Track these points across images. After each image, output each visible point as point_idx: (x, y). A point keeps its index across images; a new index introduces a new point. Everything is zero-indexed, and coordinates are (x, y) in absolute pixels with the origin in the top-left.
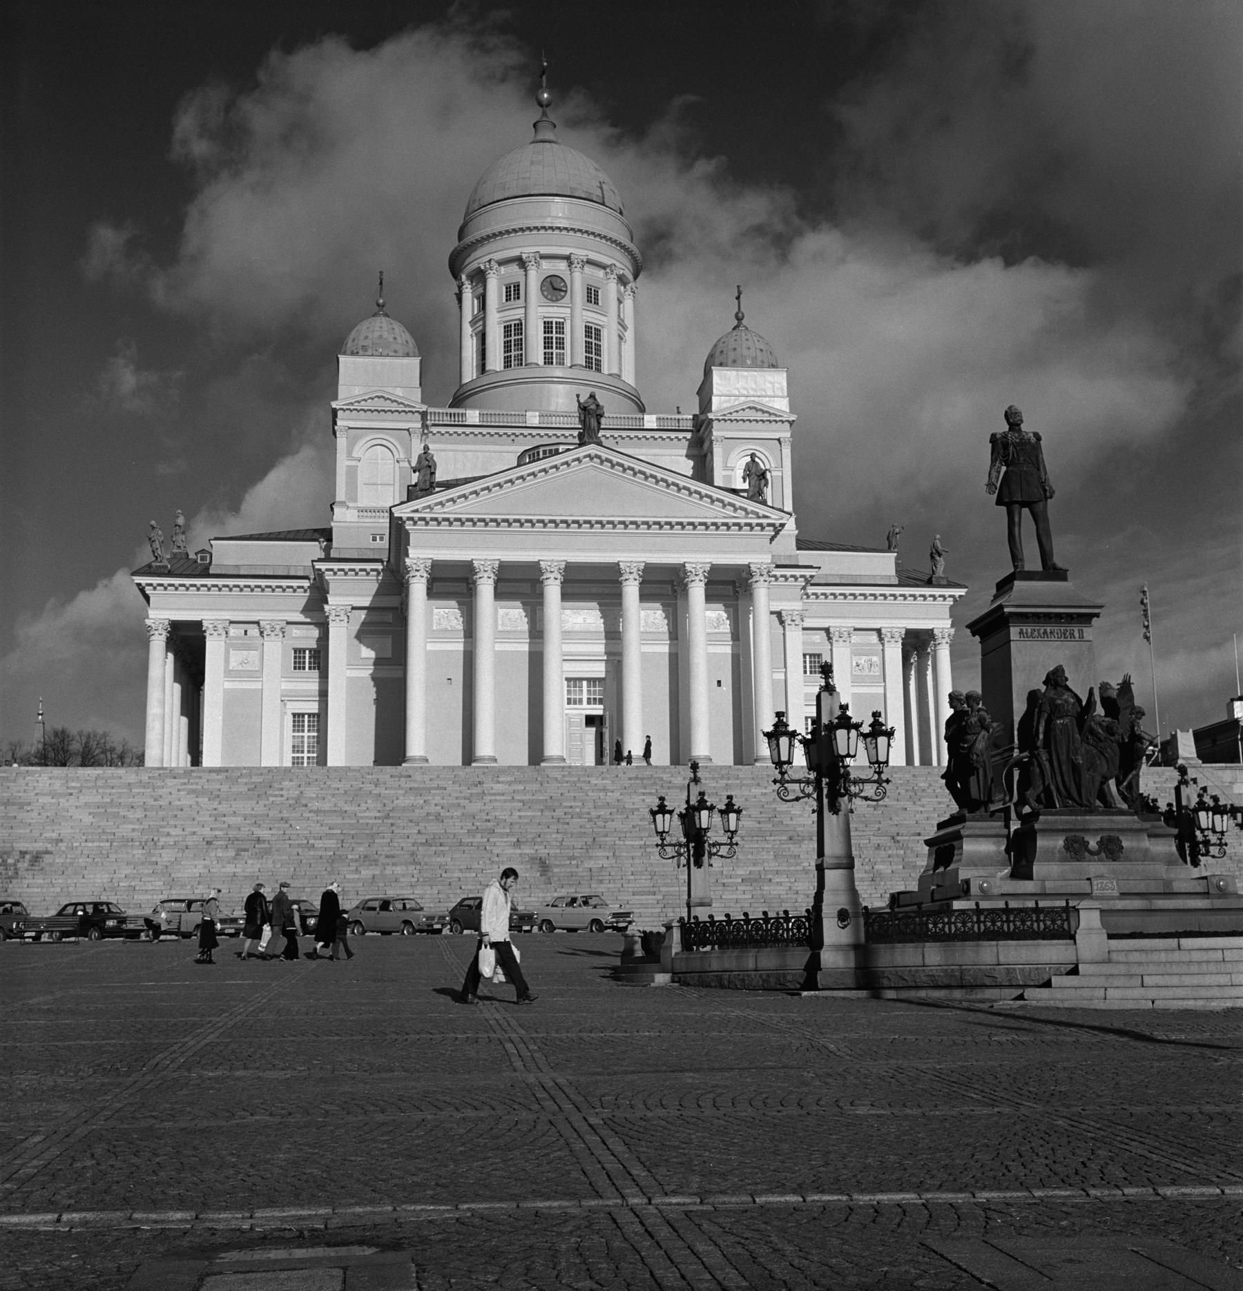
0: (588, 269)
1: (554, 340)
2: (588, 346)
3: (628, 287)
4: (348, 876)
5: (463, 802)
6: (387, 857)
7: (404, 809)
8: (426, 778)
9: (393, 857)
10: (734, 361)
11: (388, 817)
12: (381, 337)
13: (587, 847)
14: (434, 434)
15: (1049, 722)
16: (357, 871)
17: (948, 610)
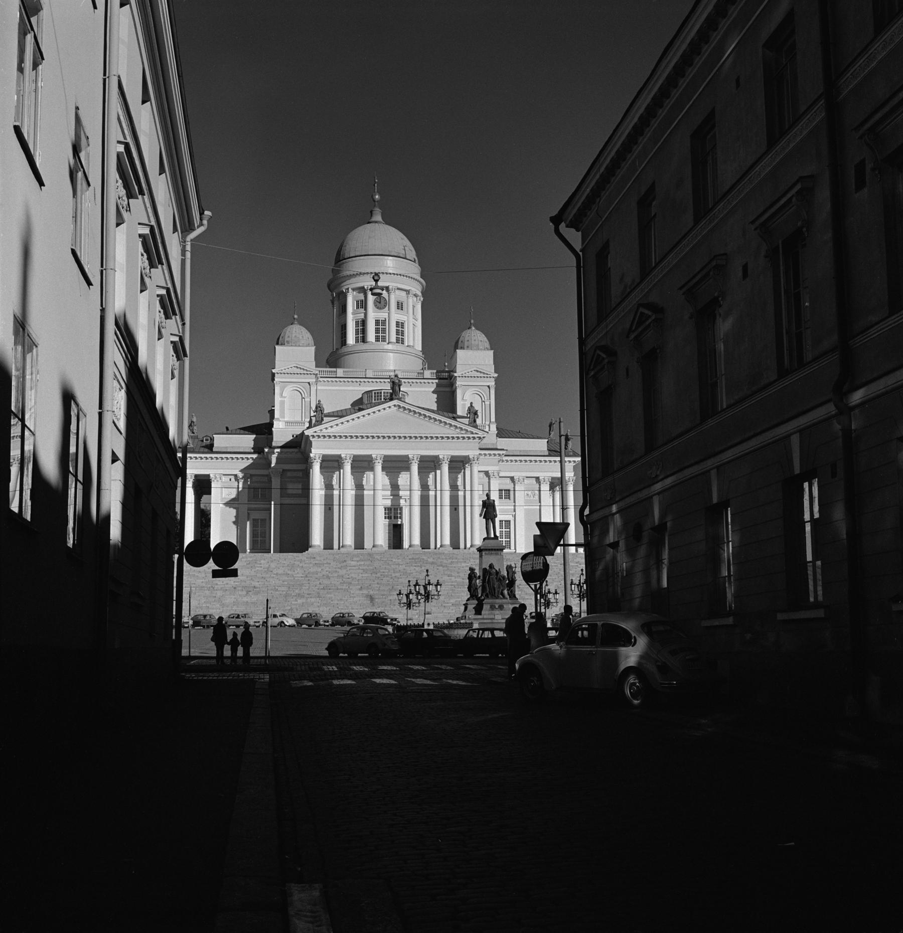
0: (397, 291)
1: (380, 329)
2: (397, 332)
3: (418, 298)
4: (293, 603)
5: (338, 570)
6: (308, 594)
7: (313, 573)
8: (322, 559)
9: (310, 594)
10: (468, 347)
11: (306, 576)
12: (295, 336)
13: (390, 590)
14: (320, 381)
15: (489, 577)
16: (296, 600)
17: (572, 467)
